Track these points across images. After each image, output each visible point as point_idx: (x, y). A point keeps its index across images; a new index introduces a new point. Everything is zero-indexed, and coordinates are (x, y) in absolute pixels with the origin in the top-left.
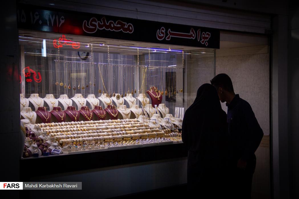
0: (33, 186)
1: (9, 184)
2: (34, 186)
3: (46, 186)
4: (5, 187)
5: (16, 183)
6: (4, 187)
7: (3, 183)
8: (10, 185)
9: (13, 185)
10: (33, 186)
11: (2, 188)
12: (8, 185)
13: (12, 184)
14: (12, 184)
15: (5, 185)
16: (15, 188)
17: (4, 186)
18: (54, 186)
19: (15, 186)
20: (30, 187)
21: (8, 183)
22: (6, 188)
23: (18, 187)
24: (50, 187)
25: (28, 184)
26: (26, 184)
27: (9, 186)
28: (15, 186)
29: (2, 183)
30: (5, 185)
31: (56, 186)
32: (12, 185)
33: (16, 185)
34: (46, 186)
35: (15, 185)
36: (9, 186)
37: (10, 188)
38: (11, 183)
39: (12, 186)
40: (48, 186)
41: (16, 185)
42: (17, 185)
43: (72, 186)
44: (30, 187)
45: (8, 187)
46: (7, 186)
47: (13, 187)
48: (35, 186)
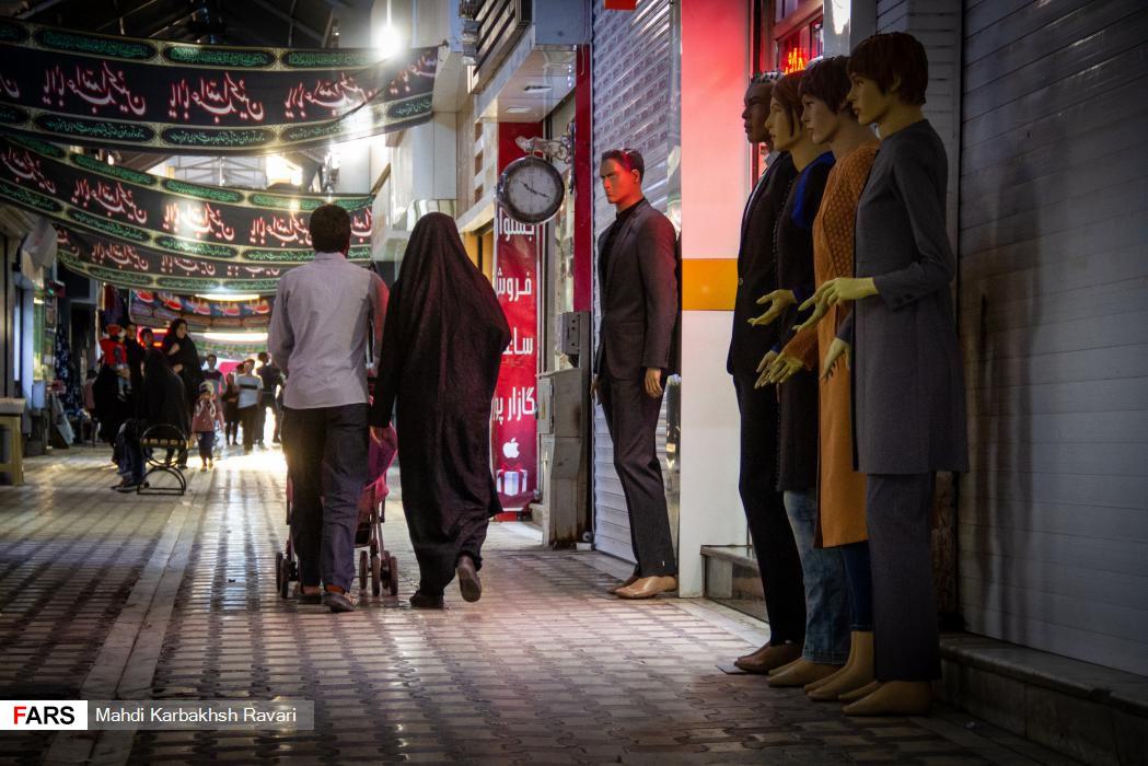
0: (126, 716)
1: (34, 709)
3: (177, 716)
4: (19, 718)
5: (59, 704)
6: (16, 722)
7: (10, 704)
8: (37, 714)
9: (51, 712)
10: (126, 716)
12: (31, 713)
13: (46, 709)
14: (46, 709)
15: (20, 711)
16: (57, 722)
17: (16, 715)
18: (207, 716)
19: (59, 716)
20: (116, 718)
21: (29, 704)
22: (22, 725)
23: (68, 719)
24: (193, 718)
25: (108, 709)
26: (98, 710)
27: (33, 715)
28: (59, 716)
29: (8, 706)
30: (20, 711)
31: (213, 716)
32: (46, 712)
33: (60, 713)
34: (177, 716)
35: (56, 713)
36: (34, 715)
37: (40, 722)
38: (40, 705)
39: (46, 715)
40: (184, 717)
41: (60, 713)
42: (67, 711)
43: (276, 716)
44: (116, 718)
45: (30, 718)
46: (27, 716)
47: (49, 719)
48: (135, 717)
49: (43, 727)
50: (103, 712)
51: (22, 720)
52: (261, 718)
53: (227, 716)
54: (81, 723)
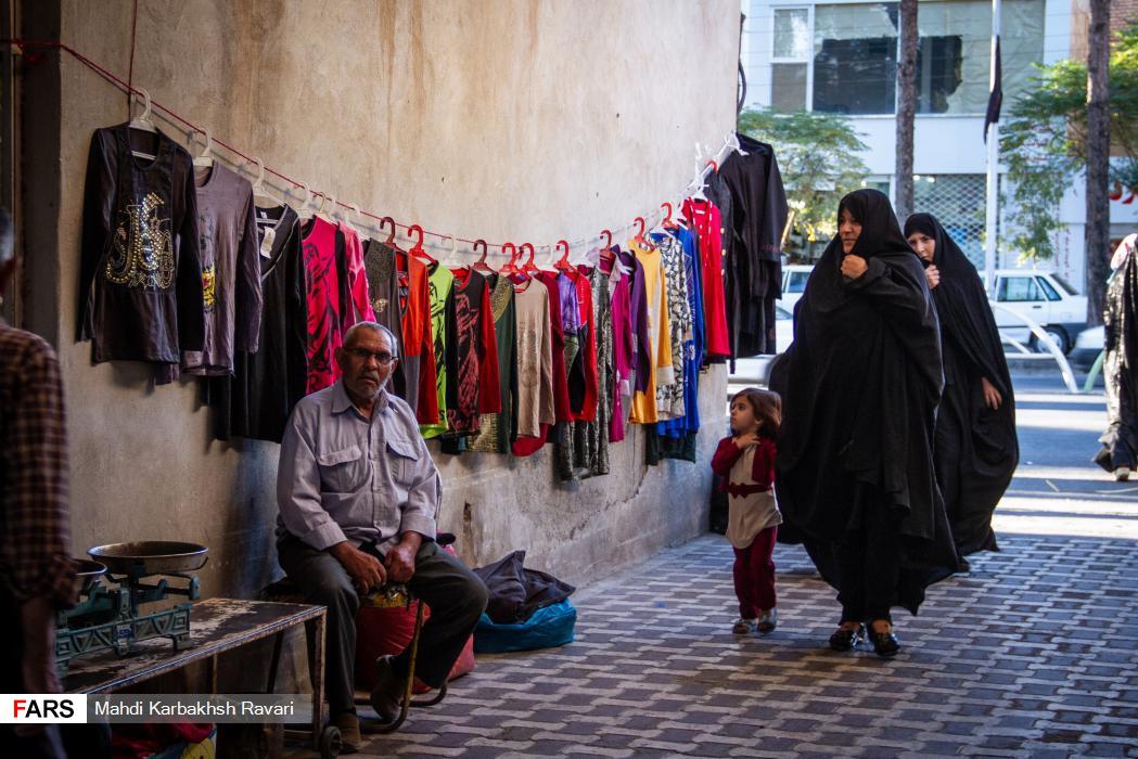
0: (125, 710)
1: (33, 703)
2: (129, 711)
3: (176, 710)
5: (59, 698)
6: (16, 715)
7: (10, 698)
8: (36, 707)
9: (51, 705)
10: (125, 710)
11: (9, 719)
12: (31, 707)
13: (46, 702)
14: (46, 702)
15: (19, 705)
16: (56, 715)
17: (16, 709)
18: (205, 710)
19: (59, 710)
20: (114, 712)
21: (29, 697)
22: (22, 719)
23: (67, 712)
24: (192, 712)
25: (107, 703)
26: (97, 703)
27: (33, 709)
28: (59, 710)
29: (8, 700)
30: (19, 705)
31: (211, 710)
32: (45, 705)
33: (59, 706)
34: (176, 710)
35: (56, 707)
36: (33, 709)
37: (39, 716)
38: (40, 698)
39: (46, 709)
40: (182, 710)
41: (59, 706)
42: (66, 704)
43: (273, 709)
44: (114, 712)
45: (30, 712)
46: (27, 710)
47: (49, 712)
48: (134, 710)
49: (42, 720)
50: (102, 706)
51: (22, 714)
52: (259, 712)
53: (225, 709)
54: (80, 717)
